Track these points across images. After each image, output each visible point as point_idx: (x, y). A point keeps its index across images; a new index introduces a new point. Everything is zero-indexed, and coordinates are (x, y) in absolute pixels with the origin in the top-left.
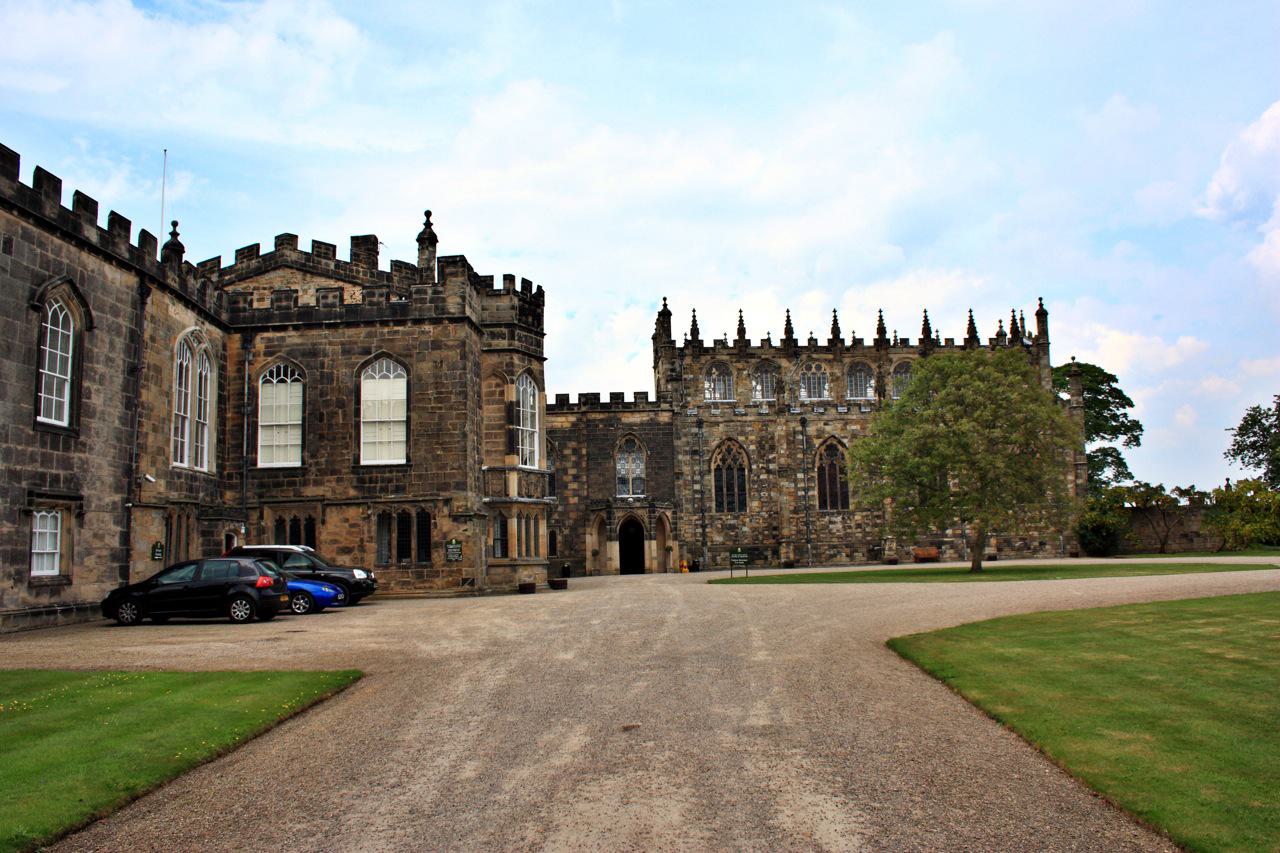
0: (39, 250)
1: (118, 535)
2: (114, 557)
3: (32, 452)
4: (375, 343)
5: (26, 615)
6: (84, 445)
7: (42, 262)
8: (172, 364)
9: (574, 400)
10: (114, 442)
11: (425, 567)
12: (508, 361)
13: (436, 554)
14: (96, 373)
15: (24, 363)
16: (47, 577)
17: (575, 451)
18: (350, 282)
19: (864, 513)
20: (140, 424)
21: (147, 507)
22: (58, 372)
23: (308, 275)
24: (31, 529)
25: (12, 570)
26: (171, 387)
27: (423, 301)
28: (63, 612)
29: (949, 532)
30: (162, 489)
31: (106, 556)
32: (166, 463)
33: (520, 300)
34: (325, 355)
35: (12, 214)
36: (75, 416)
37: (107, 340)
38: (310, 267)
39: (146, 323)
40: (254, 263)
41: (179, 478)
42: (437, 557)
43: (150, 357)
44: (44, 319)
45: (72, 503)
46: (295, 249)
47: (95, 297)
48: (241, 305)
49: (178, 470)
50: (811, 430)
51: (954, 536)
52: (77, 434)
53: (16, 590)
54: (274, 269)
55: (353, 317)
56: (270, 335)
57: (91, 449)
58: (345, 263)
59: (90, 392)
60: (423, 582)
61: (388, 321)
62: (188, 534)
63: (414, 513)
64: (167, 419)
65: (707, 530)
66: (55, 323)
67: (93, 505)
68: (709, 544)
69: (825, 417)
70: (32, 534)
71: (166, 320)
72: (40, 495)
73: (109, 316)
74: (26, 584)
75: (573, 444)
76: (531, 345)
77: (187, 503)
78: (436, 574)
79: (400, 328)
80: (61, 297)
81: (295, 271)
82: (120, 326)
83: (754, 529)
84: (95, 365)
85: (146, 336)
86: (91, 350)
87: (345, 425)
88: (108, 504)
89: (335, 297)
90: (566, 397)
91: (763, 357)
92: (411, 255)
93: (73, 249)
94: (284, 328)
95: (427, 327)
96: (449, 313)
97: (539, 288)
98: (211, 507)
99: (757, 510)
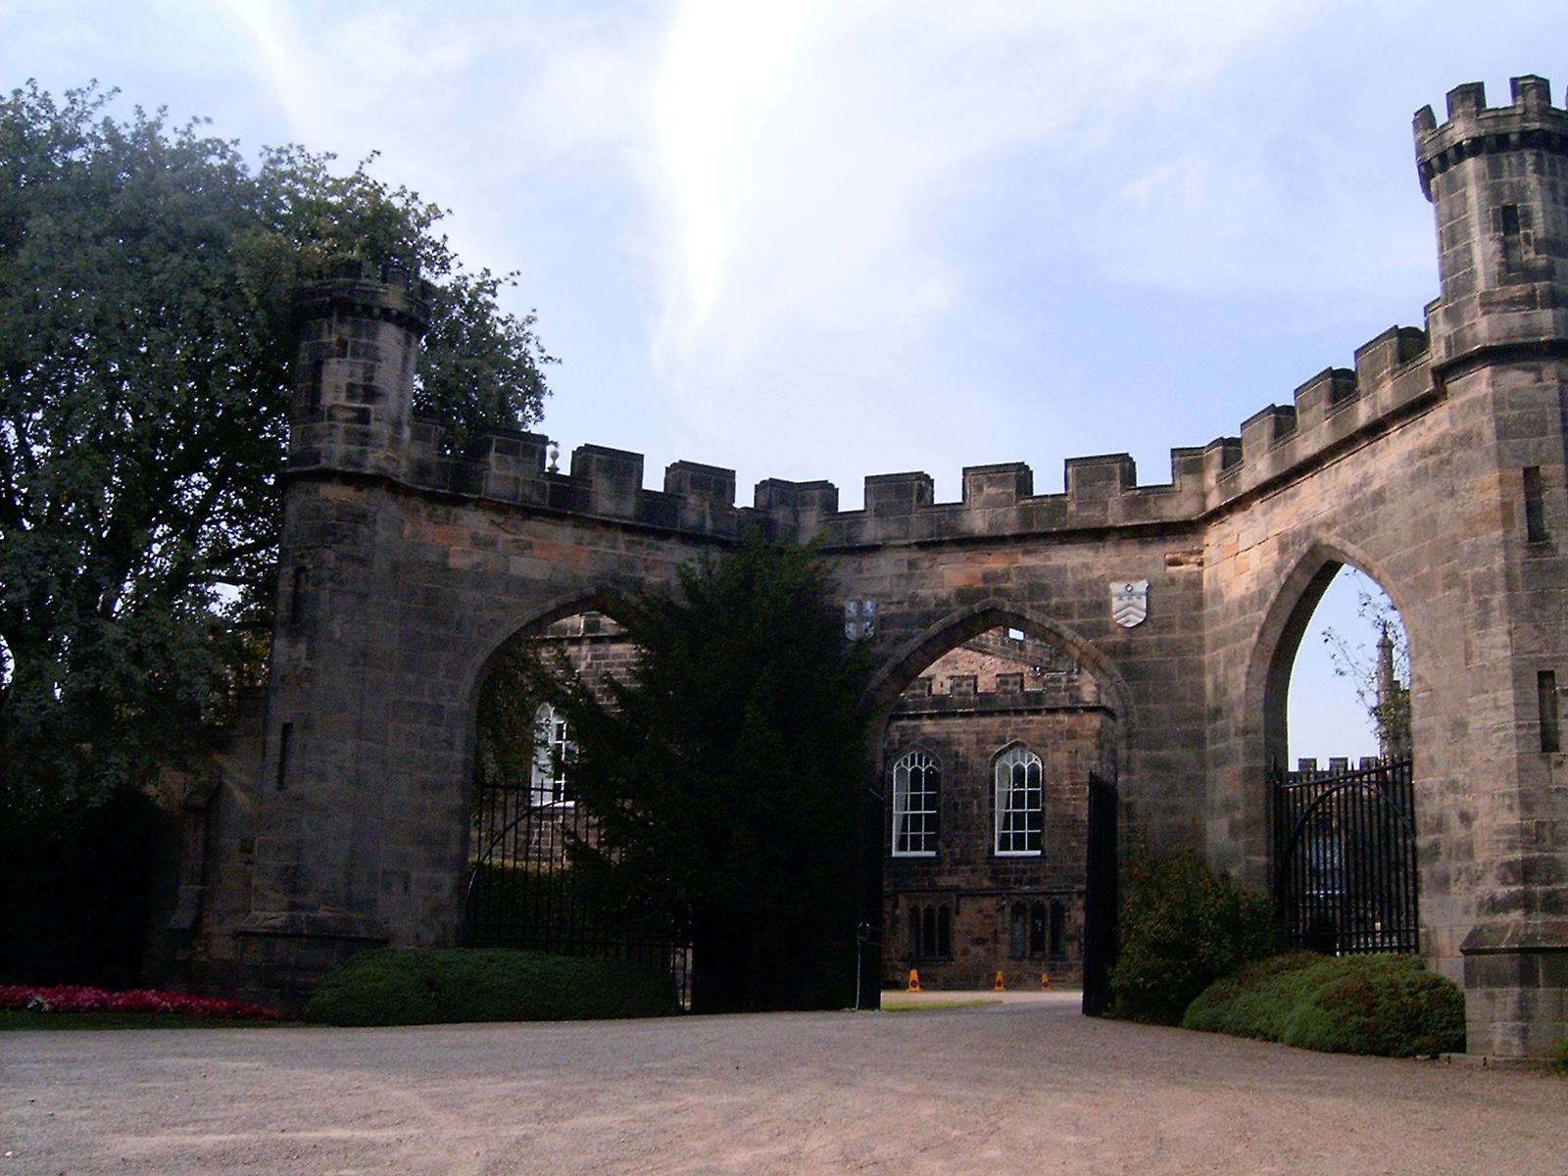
4: (1010, 731)
11: (1058, 959)
13: (1070, 947)
27: (1058, 689)
34: (960, 744)
56: (904, 723)
60: (1055, 975)
63: (1047, 904)
78: (1070, 967)
79: (1036, 718)
87: (979, 816)
89: (969, 685)
94: (919, 717)
95: (1062, 717)
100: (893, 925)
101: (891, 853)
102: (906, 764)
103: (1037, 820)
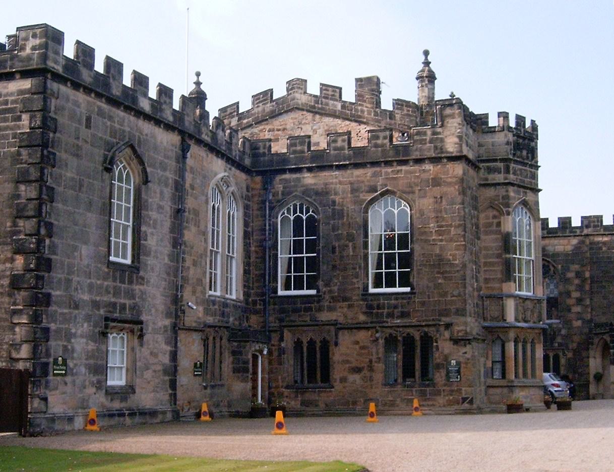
0: (109, 123)
1: (168, 353)
2: (165, 372)
3: (107, 286)
4: (380, 181)
5: (105, 416)
6: (143, 279)
7: (111, 133)
8: (207, 207)
9: (576, 223)
10: (165, 276)
11: (428, 386)
12: (504, 194)
13: (438, 374)
14: (150, 219)
15: (101, 214)
16: (117, 386)
17: (578, 275)
18: (356, 121)
20: (184, 260)
21: (189, 329)
22: (122, 220)
23: (318, 116)
24: (107, 347)
25: (94, 379)
26: (206, 227)
27: (423, 142)
28: (130, 415)
30: (201, 315)
31: (159, 371)
32: (204, 293)
33: (514, 135)
34: (336, 194)
35: (91, 97)
36: (136, 257)
37: (158, 191)
38: (319, 109)
39: (187, 174)
40: (269, 107)
41: (214, 304)
42: (439, 377)
43: (190, 203)
44: (112, 178)
45: (134, 326)
46: (305, 93)
47: (149, 155)
48: (261, 151)
49: (213, 298)
52: (138, 269)
53: (97, 395)
54: (286, 112)
55: (359, 159)
56: (287, 176)
57: (148, 282)
58: (351, 103)
59: (146, 235)
60: (425, 400)
61: (392, 161)
62: (221, 354)
63: (417, 336)
64: (203, 255)
66: (120, 180)
67: (150, 328)
70: (107, 351)
71: (202, 170)
72: (114, 320)
73: (159, 171)
74: (104, 391)
75: (576, 267)
76: (526, 177)
77: (220, 327)
78: (438, 393)
79: (404, 168)
80: (125, 159)
81: (305, 113)
82: (168, 178)
84: (150, 213)
85: (187, 185)
86: (147, 201)
87: (355, 256)
88: (161, 328)
89: (343, 141)
90: (569, 219)
92: (413, 94)
93: (132, 118)
94: (299, 170)
95: (428, 166)
96: (447, 152)
97: (533, 122)
98: (240, 330)
100: (280, 355)
101: (276, 292)
102: (289, 212)
103: (406, 260)
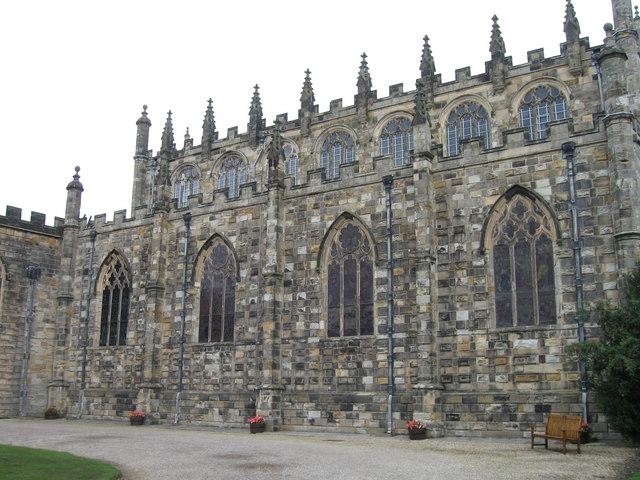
19: (248, 347)
29: (367, 380)
50: (196, 229)
51: (376, 388)
65: (87, 368)
68: (87, 385)
69: (212, 209)
83: (127, 368)
91: (227, 149)
99: (133, 343)
